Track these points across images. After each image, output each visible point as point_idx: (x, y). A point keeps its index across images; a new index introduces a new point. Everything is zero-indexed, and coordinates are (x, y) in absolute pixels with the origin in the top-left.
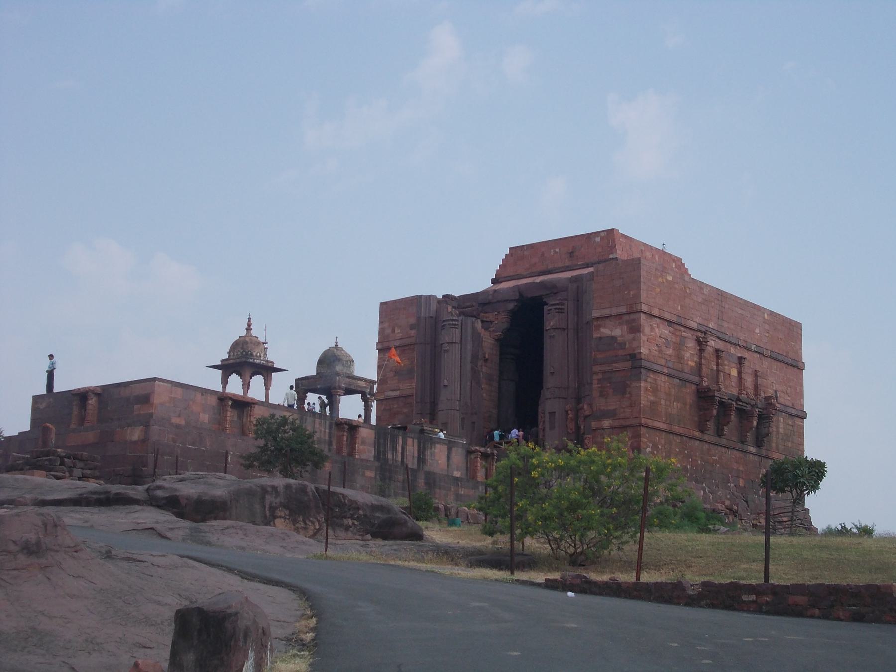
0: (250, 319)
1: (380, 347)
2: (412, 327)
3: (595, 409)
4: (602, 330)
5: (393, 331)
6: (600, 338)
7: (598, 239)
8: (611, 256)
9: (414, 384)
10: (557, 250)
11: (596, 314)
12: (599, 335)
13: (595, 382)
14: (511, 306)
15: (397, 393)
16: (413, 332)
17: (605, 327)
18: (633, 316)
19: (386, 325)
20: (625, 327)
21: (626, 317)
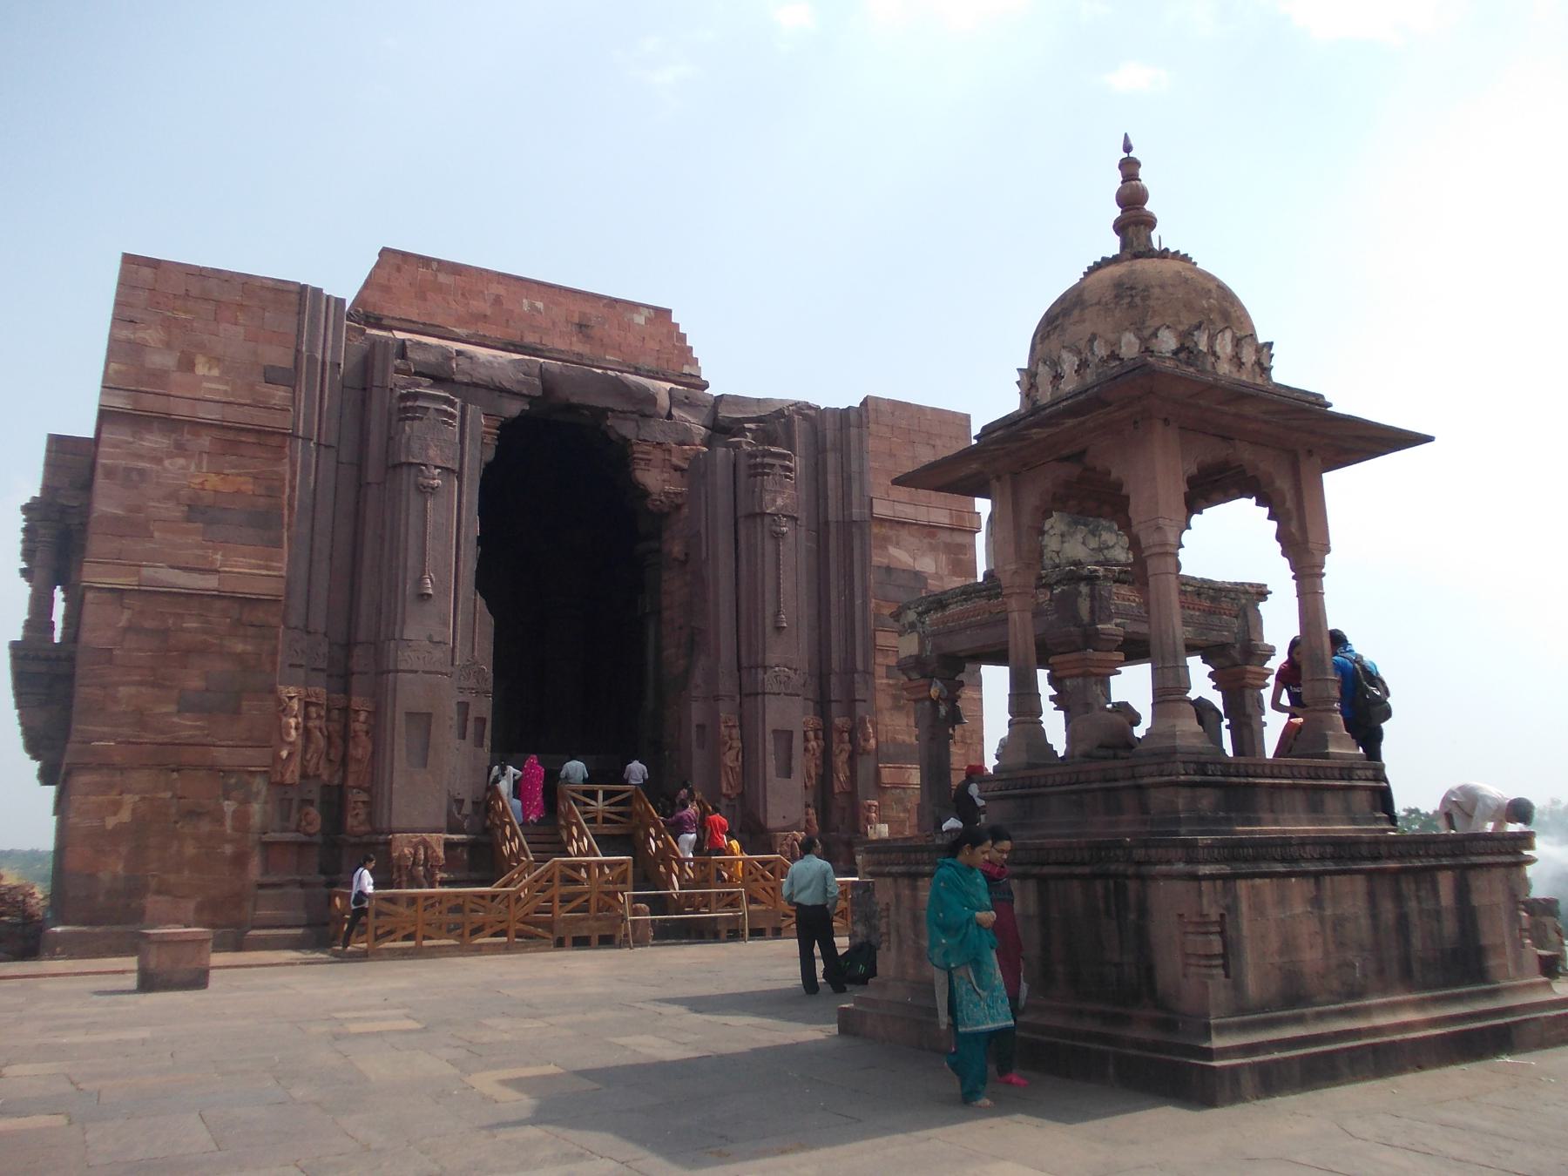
0: (1129, 168)
1: (119, 402)
2: (272, 376)
3: (882, 739)
4: (893, 550)
5: (187, 365)
6: (888, 569)
7: (640, 319)
8: (687, 369)
9: (282, 566)
10: (540, 305)
11: (881, 509)
12: (886, 561)
13: (881, 671)
14: (514, 408)
15: (210, 582)
16: (280, 394)
17: (897, 545)
18: (959, 538)
19: (152, 335)
20: (943, 558)
21: (944, 537)
